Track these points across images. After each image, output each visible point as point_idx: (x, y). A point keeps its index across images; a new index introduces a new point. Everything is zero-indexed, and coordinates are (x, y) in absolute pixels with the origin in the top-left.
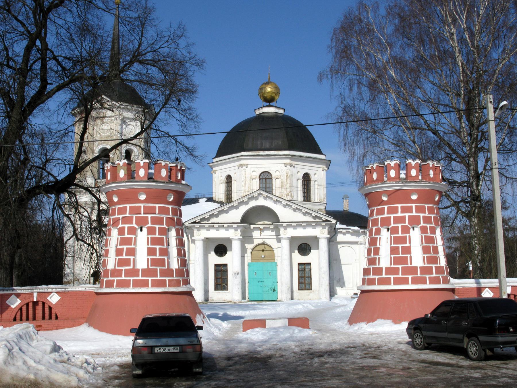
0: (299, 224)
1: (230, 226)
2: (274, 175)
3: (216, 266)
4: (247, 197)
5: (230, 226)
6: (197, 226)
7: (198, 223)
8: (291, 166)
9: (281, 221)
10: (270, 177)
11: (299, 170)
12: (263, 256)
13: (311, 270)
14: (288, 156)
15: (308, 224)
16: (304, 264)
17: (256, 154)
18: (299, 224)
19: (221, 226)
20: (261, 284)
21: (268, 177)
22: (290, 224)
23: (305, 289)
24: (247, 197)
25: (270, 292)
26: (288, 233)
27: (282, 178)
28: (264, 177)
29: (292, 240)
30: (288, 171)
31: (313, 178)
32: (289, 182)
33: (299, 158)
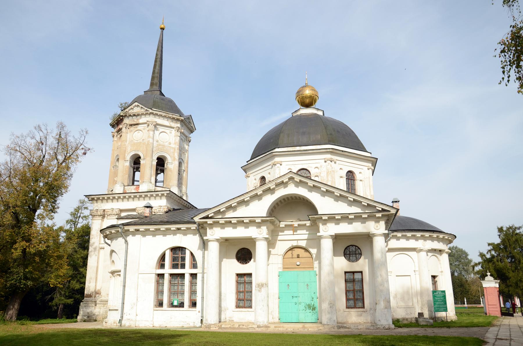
0: (345, 218)
1: (252, 222)
4: (274, 183)
5: (252, 222)
6: (210, 221)
7: (211, 218)
8: (331, 161)
11: (342, 167)
13: (362, 281)
14: (328, 150)
15: (358, 217)
17: (291, 150)
18: (345, 218)
19: (241, 222)
20: (295, 300)
22: (332, 218)
24: (274, 183)
25: (308, 311)
26: (329, 230)
27: (321, 175)
29: (337, 238)
30: (329, 166)
31: (358, 176)
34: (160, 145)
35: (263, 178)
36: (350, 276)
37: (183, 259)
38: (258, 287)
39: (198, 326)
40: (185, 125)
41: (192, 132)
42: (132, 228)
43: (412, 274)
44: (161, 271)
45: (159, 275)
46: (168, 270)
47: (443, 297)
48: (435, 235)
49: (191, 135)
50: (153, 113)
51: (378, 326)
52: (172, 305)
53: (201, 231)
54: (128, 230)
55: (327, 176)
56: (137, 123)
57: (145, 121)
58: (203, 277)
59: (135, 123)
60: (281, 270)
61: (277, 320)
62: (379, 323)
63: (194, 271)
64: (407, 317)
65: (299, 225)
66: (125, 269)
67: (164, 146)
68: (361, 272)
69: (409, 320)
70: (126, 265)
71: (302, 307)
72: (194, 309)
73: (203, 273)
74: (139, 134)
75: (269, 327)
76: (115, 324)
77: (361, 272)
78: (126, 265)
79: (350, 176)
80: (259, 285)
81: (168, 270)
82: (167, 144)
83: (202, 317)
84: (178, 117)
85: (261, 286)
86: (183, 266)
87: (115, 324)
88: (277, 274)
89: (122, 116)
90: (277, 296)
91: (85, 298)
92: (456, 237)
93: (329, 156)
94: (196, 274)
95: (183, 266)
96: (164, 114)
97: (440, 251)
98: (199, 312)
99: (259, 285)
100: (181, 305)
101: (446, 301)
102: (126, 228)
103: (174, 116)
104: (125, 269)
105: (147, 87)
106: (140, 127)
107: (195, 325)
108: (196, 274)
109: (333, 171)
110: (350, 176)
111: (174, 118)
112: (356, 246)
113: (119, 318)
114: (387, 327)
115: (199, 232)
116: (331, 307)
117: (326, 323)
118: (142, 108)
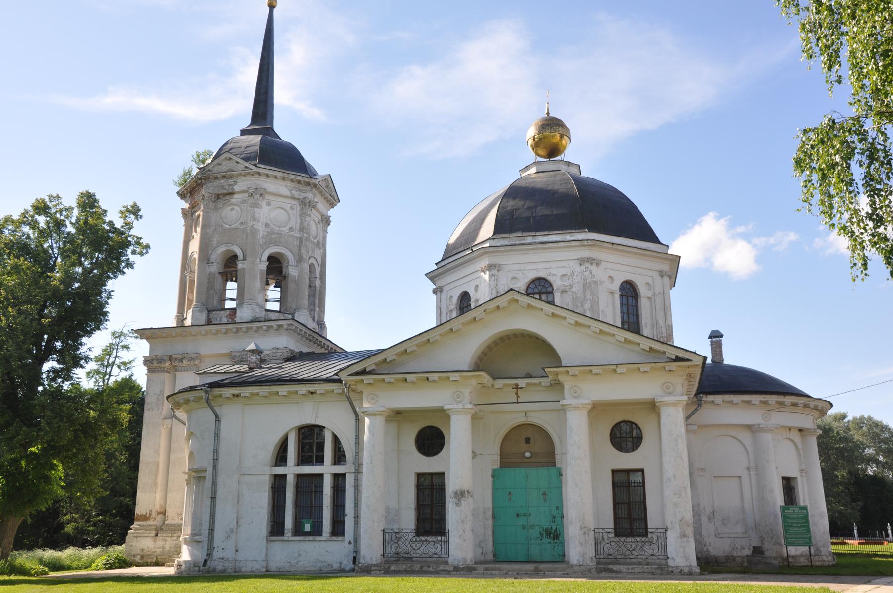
2: (557, 283)
3: (419, 475)
7: (370, 373)
9: (564, 363)
10: (549, 289)
11: (611, 273)
12: (528, 454)
13: (644, 486)
14: (586, 243)
16: (628, 471)
20: (522, 521)
21: (544, 290)
23: (631, 534)
25: (546, 540)
27: (574, 289)
28: (536, 290)
30: (587, 273)
31: (643, 291)
32: (589, 297)
33: (610, 246)
34: (273, 233)
35: (465, 297)
36: (621, 478)
37: (321, 447)
38: (455, 497)
39: (347, 569)
40: (320, 193)
41: (333, 205)
42: (227, 392)
43: (744, 474)
44: (280, 470)
45: (276, 477)
46: (291, 469)
47: (802, 518)
48: (789, 399)
49: (332, 213)
50: (259, 173)
51: (670, 569)
52: (298, 531)
53: (353, 396)
54: (221, 396)
55: (584, 292)
56: (230, 191)
57: (245, 188)
58: (356, 480)
59: (225, 192)
60: (497, 466)
61: (490, 557)
62: (671, 563)
63: (339, 469)
64: (735, 554)
65: (528, 384)
66: (215, 467)
67: (280, 234)
68: (642, 470)
69: (739, 560)
70: (216, 460)
71: (535, 533)
72: (340, 538)
73: (358, 471)
74: (233, 212)
75: (475, 569)
76: (197, 569)
77: (642, 470)
78: (216, 460)
79: (629, 291)
80: (456, 494)
81: (291, 469)
82: (285, 229)
83: (356, 552)
84: (307, 180)
85: (461, 495)
86: (320, 460)
87: (197, 569)
88: (490, 473)
89: (201, 179)
90: (490, 513)
91: (136, 523)
92: (832, 405)
93: (585, 253)
94: (343, 475)
95: (320, 460)
96: (279, 174)
97: (800, 430)
98: (350, 543)
99: (456, 494)
100: (317, 531)
101: (808, 526)
102: (217, 391)
103: (299, 178)
104: (215, 467)
105: (246, 122)
106: (237, 198)
107: (343, 566)
108: (344, 475)
109: (596, 282)
110: (629, 291)
111: (299, 182)
112: (632, 423)
113: (205, 557)
114: (686, 570)
115: (349, 398)
116: (585, 533)
117: (576, 562)
118: (237, 162)
